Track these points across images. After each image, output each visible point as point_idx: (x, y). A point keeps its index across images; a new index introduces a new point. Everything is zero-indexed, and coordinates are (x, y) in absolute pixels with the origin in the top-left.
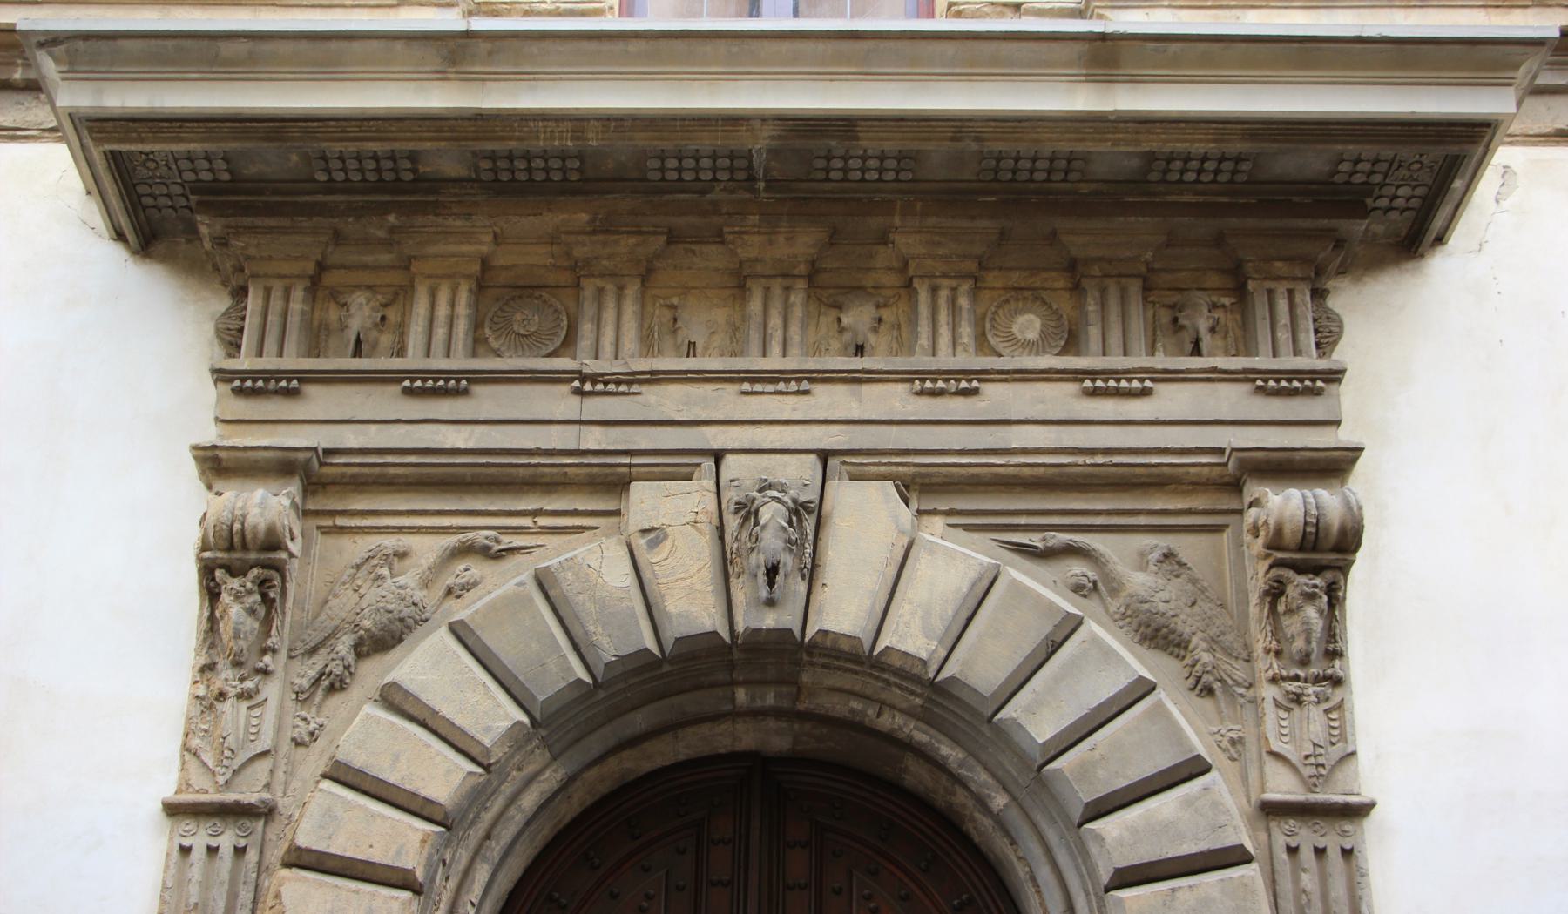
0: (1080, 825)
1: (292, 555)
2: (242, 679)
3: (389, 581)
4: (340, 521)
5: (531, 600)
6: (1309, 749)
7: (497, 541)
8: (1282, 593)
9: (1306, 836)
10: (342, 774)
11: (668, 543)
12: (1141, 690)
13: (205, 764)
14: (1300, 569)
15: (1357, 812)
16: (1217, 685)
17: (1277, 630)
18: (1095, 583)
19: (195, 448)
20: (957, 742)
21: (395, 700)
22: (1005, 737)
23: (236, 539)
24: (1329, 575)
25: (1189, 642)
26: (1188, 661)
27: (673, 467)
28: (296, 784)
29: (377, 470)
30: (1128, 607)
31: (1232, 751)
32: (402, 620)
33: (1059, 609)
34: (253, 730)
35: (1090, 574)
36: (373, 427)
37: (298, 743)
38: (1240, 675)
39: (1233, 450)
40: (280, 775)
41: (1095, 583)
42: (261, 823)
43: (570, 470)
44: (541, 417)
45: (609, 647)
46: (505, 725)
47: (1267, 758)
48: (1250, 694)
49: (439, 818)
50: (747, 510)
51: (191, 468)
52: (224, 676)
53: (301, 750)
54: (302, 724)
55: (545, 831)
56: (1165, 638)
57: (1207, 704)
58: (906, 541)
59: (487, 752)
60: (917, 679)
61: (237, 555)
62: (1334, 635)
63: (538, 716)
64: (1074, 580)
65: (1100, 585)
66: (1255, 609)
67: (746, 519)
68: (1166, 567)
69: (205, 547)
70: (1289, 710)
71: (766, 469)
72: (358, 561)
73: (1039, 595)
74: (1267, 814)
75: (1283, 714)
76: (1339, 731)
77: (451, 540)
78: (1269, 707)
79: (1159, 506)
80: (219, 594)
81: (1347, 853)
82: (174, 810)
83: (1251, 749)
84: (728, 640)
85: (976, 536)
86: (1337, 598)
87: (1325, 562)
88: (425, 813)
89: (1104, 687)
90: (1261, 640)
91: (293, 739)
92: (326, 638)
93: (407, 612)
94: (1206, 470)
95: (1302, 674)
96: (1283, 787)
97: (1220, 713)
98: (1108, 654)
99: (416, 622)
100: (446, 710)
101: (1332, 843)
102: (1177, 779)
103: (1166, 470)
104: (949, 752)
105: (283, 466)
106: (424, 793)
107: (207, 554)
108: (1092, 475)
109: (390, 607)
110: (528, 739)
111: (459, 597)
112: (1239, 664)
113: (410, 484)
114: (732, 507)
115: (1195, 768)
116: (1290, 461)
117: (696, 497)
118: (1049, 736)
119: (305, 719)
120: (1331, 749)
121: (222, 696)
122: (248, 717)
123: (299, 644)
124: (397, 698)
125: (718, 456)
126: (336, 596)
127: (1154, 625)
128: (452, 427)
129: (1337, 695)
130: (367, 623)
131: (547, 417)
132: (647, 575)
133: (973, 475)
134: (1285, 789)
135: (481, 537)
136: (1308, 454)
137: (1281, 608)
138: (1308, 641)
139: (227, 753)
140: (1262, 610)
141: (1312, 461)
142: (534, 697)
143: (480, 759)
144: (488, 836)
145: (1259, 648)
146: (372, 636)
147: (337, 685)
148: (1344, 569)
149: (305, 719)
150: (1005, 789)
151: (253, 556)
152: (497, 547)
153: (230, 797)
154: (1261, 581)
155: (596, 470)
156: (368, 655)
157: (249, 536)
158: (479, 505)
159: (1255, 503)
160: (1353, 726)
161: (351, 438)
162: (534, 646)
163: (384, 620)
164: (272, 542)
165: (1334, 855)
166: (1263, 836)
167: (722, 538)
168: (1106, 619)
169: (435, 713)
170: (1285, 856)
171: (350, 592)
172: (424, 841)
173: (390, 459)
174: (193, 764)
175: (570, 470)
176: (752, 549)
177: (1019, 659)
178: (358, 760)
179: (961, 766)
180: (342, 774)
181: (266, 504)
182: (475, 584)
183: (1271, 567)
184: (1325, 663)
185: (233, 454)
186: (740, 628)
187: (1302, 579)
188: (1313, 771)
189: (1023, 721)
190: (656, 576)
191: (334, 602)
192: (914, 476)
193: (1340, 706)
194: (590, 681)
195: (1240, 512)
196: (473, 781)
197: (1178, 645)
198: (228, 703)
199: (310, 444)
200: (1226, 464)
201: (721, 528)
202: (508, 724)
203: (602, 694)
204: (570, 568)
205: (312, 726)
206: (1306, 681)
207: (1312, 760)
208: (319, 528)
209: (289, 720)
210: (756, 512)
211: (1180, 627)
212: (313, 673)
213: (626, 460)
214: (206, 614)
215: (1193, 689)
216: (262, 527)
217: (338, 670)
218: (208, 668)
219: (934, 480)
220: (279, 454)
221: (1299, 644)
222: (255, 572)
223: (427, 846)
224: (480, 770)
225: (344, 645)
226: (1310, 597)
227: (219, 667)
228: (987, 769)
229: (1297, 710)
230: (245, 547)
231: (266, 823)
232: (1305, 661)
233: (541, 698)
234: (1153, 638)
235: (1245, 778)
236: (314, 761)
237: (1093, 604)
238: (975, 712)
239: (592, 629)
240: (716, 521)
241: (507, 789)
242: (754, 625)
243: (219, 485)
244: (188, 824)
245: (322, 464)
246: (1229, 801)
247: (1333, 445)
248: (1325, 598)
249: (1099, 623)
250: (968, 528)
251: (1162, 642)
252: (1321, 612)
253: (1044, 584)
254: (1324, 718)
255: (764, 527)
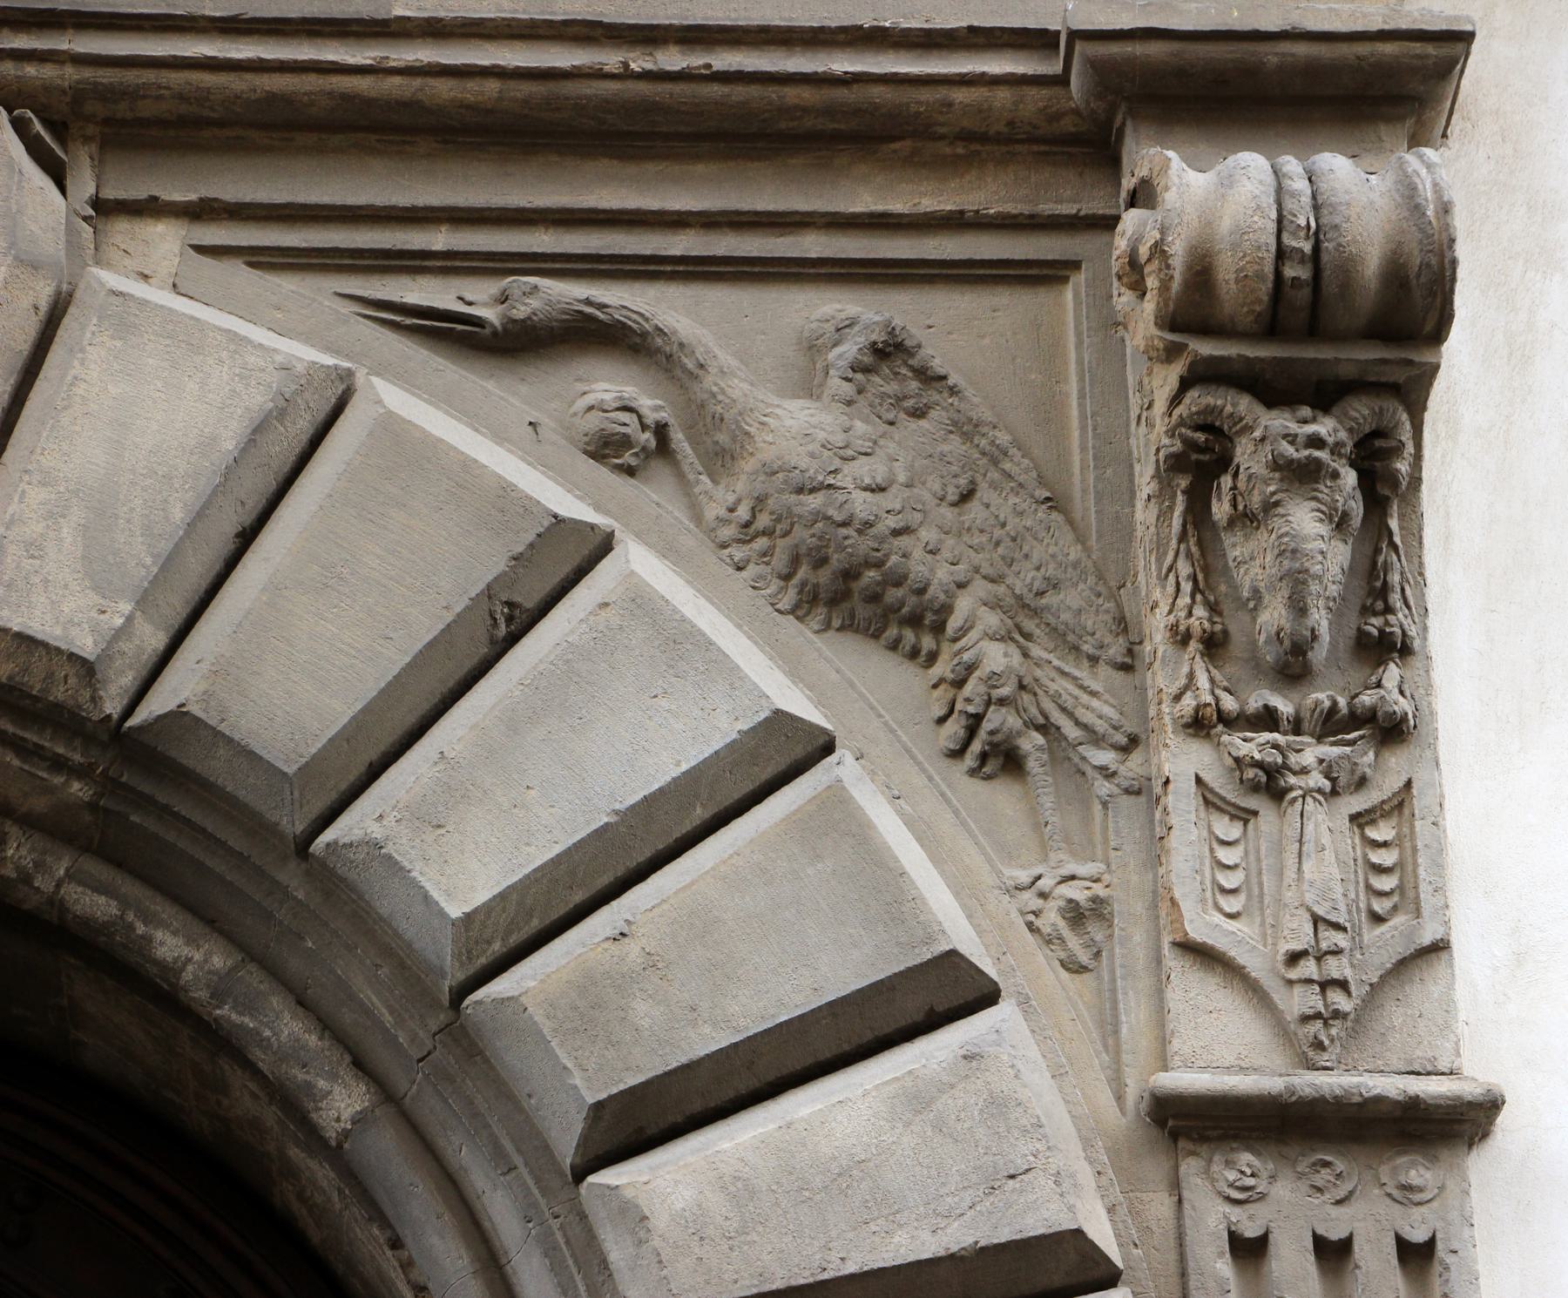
0: (580, 1175)
6: (1300, 935)
8: (1224, 462)
9: (1291, 1204)
12: (784, 754)
14: (1274, 389)
15: (1450, 1126)
16: (1031, 743)
17: (1208, 576)
18: (661, 431)
20: (209, 919)
22: (346, 900)
24: (1361, 409)
25: (946, 610)
26: (941, 669)
30: (760, 502)
31: (1074, 942)
33: (528, 506)
35: (646, 403)
38: (1101, 711)
39: (1075, 35)
41: (661, 431)
47: (1174, 963)
48: (1133, 766)
56: (874, 598)
57: (1001, 796)
58: (43, 293)
60: (65, 720)
62: (1385, 590)
64: (594, 422)
65: (678, 437)
66: (1150, 515)
68: (880, 384)
70: (1245, 816)
73: (469, 465)
74: (1175, 1136)
75: (1227, 829)
76: (1396, 873)
78: (1182, 805)
79: (864, 202)
81: (1416, 1256)
83: (1131, 937)
85: (287, 285)
86: (1393, 480)
87: (1348, 372)
89: (661, 743)
90: (1161, 607)
94: (1003, 95)
95: (1284, 706)
96: (1224, 1051)
97: (1039, 826)
98: (680, 642)
101: (1371, 1223)
102: (888, 1028)
103: (877, 93)
104: (179, 948)
108: (650, 108)
112: (1102, 678)
115: (944, 993)
116: (1251, 71)
118: (482, 896)
120: (1371, 934)
127: (837, 560)
129: (1392, 770)
133: (272, 98)
134: (1230, 1059)
136: (1302, 49)
137: (1220, 510)
138: (1299, 609)
140: (1164, 515)
141: (1312, 70)
145: (1157, 626)
148: (1412, 392)
150: (361, 1065)
154: (1160, 427)
159: (1143, 196)
160: (1439, 866)
165: (1375, 1261)
166: (1159, 1206)
168: (691, 540)
170: (1224, 1267)
177: (396, 658)
179: (219, 996)
183: (1185, 384)
184: (1356, 676)
187: (1278, 421)
188: (1310, 1000)
189: (404, 849)
192: (78, 95)
193: (1400, 804)
195: (1108, 223)
197: (915, 621)
200: (1062, 80)
206: (1297, 727)
207: (1309, 968)
211: (918, 567)
215: (957, 754)
219: (147, 109)
221: (1274, 615)
226: (1303, 475)
228: (302, 1002)
229: (1267, 814)
232: (1293, 667)
234: (836, 599)
235: (1109, 1027)
237: (653, 495)
238: (259, 827)
246: (1040, 1091)
247: (1376, 25)
248: (1350, 478)
249: (668, 551)
250: (262, 259)
251: (863, 612)
252: (1340, 523)
253: (500, 437)
254: (1349, 842)
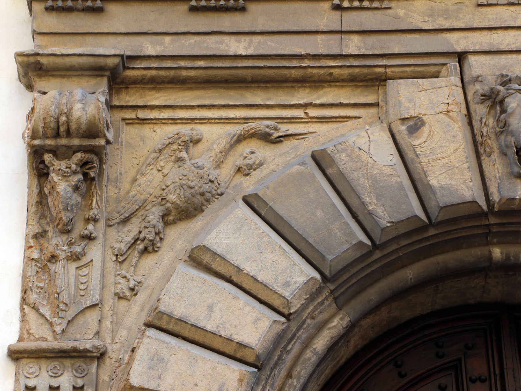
1: (108, 142)
2: (70, 244)
3: (188, 163)
4: (142, 114)
5: (313, 177)
7: (276, 129)
10: (164, 324)
11: (426, 129)
13: (43, 316)
19: (19, 55)
21: (201, 260)
23: (62, 129)
27: (423, 67)
28: (123, 332)
29: (172, 73)
32: (202, 194)
34: (82, 287)
36: (168, 39)
37: (120, 297)
40: (107, 323)
42: (95, 365)
43: (336, 71)
44: (308, 29)
45: (384, 215)
46: (303, 279)
49: (251, 359)
50: (494, 100)
51: (11, 69)
52: (54, 242)
53: (123, 303)
54: (123, 281)
55: (327, 371)
59: (288, 303)
61: (63, 141)
63: (327, 273)
67: (492, 107)
69: (34, 136)
71: (505, 67)
72: (160, 146)
77: (237, 129)
80: (47, 175)
82: (15, 355)
84: (485, 208)
88: (238, 356)
91: (116, 294)
92: (137, 210)
93: (207, 187)
99: (213, 196)
100: (249, 268)
105: (95, 69)
106: (237, 338)
107: (37, 142)
109: (192, 184)
110: (319, 291)
111: (248, 175)
113: (200, 83)
114: (478, 98)
117: (446, 91)
119: (125, 277)
121: (53, 258)
122: (77, 277)
123: (116, 215)
124: (206, 258)
125: (461, 57)
126: (143, 174)
128: (233, 38)
130: (172, 197)
131: (314, 29)
132: (410, 155)
135: (263, 126)
139: (62, 306)
142: (323, 257)
143: (281, 309)
144: (289, 375)
146: (177, 207)
147: (150, 249)
149: (125, 277)
151: (76, 142)
152: (276, 134)
153: (67, 344)
155: (357, 70)
156: (174, 222)
157: (73, 127)
158: (259, 101)
161: (149, 47)
162: (319, 213)
163: (188, 194)
164: (92, 132)
167: (470, 124)
169: (239, 270)
171: (155, 171)
172: (240, 380)
173: (183, 63)
174: (32, 316)
175: (336, 71)
176: (502, 132)
178: (179, 310)
180: (164, 324)
181: (84, 101)
182: (261, 164)
185: (52, 59)
186: (495, 197)
190: (417, 156)
191: (142, 180)
194: (369, 243)
196: (279, 328)
198: (60, 264)
199: (117, 52)
201: (469, 115)
202: (304, 279)
203: (378, 255)
204: (344, 150)
205: (132, 284)
208: (124, 119)
209: (111, 279)
210: (502, 102)
212: (129, 239)
213: (382, 62)
214: (36, 191)
216: (84, 119)
217: (151, 237)
218: (39, 236)
220: (91, 60)
222: (79, 155)
223: (244, 384)
224: (283, 319)
225: (154, 215)
227: (50, 234)
230: (69, 134)
231: (98, 366)
233: (330, 257)
236: (135, 312)
239: (367, 200)
240: (464, 111)
241: (303, 334)
242: (507, 194)
243: (40, 84)
244: (30, 366)
245: (125, 68)
255: (511, 114)
